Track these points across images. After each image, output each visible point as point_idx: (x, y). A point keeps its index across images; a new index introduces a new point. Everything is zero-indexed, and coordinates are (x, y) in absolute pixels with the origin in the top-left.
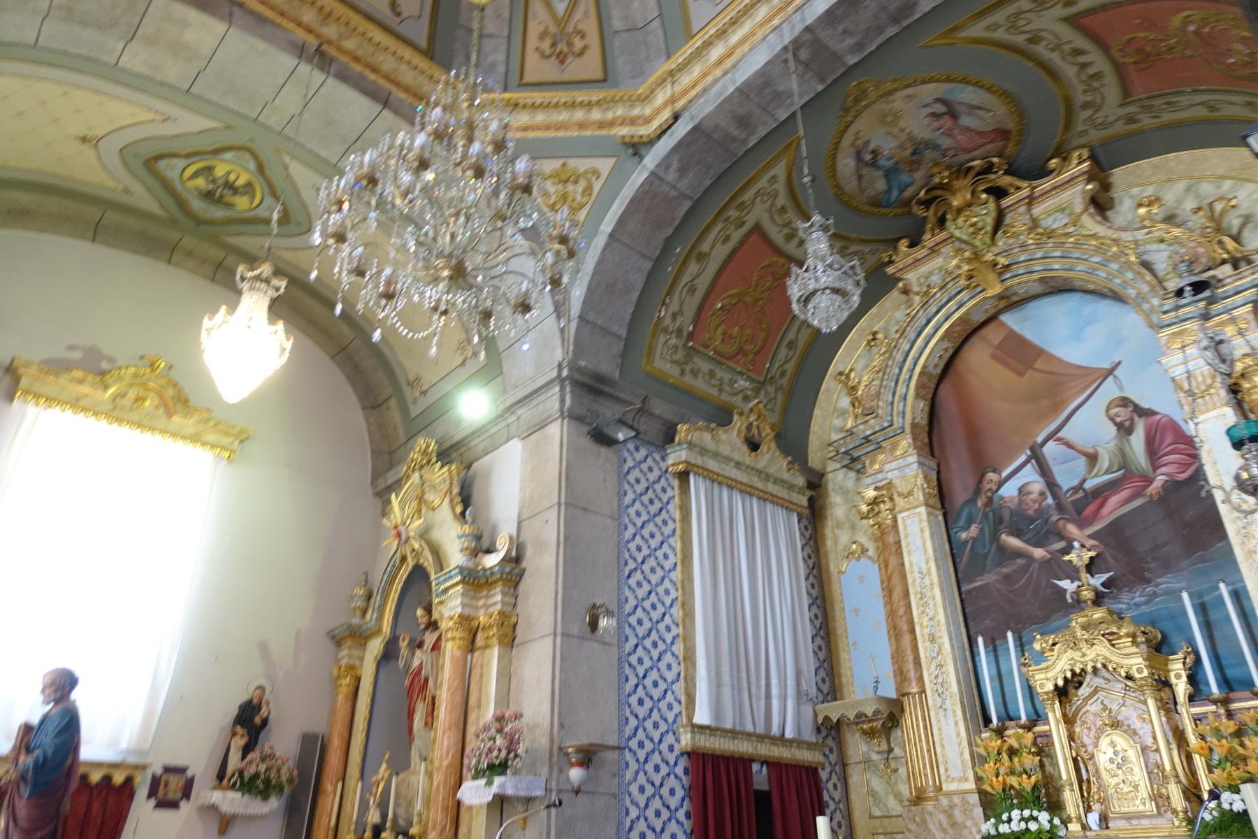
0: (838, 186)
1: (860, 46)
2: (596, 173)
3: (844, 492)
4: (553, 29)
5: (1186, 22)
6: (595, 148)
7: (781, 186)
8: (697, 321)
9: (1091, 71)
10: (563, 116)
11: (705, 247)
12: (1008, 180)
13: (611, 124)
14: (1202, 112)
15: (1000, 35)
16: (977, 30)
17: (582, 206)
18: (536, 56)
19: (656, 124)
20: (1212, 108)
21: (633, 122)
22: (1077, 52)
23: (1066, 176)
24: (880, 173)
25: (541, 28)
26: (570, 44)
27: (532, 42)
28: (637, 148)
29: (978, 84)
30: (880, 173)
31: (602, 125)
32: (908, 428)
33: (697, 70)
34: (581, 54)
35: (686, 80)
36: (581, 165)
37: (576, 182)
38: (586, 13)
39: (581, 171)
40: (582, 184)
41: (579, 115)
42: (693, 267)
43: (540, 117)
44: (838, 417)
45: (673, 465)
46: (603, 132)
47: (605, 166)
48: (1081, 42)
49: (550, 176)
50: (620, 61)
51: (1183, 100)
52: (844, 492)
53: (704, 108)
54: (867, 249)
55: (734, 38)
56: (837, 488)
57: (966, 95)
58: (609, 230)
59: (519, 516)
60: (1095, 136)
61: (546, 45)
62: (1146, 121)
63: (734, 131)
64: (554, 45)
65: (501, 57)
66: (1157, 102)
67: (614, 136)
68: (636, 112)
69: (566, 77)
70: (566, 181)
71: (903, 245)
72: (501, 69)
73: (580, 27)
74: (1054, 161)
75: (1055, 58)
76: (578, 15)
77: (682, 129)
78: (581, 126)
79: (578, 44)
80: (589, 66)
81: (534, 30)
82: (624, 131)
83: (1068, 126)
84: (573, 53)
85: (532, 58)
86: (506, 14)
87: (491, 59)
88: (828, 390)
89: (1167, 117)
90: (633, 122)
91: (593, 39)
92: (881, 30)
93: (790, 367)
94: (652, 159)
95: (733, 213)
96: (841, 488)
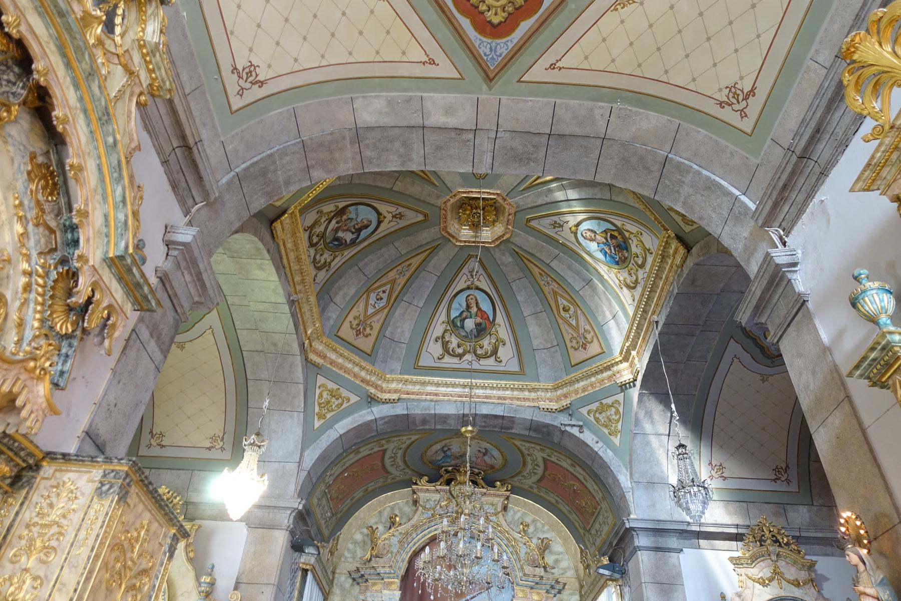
0: (426, 452)
1: (485, 427)
2: (349, 400)
3: (343, 589)
4: (362, 317)
5: (574, 485)
6: (355, 390)
7: (408, 442)
8: (334, 480)
9: (535, 471)
10: (350, 366)
11: (361, 450)
12: (482, 482)
13: (367, 383)
14: (554, 501)
15: (523, 448)
16: (518, 443)
17: (333, 410)
18: (349, 325)
19: (387, 396)
21: (376, 387)
22: (537, 465)
23: (500, 493)
24: (443, 455)
25: (358, 314)
26: (364, 329)
27: (350, 317)
28: (372, 400)
29: (501, 453)
30: (443, 455)
31: (363, 380)
32: (400, 577)
33: (417, 388)
34: (367, 336)
35: (410, 387)
36: (344, 393)
37: (337, 399)
38: (378, 320)
39: (343, 395)
40: (340, 401)
41: (356, 369)
42: (352, 456)
43: (340, 360)
44: (352, 543)
45: (304, 563)
46: (364, 385)
47: (354, 399)
48: (541, 464)
49: (329, 391)
50: (381, 350)
52: (343, 589)
53: (417, 411)
54: (410, 473)
55: (443, 390)
56: (339, 584)
57: (496, 453)
58: (342, 432)
59: (237, 579)
60: (517, 484)
61: (355, 323)
62: (535, 491)
63: (417, 422)
64: (358, 325)
65: (334, 316)
67: (368, 391)
68: (379, 383)
69: (355, 343)
70: (334, 396)
71: (426, 478)
72: (332, 322)
73: (373, 324)
74: (498, 483)
75: (530, 462)
76: (375, 319)
77: (400, 410)
78: (355, 376)
79: (368, 331)
80: (366, 344)
81: (354, 312)
82: (372, 390)
83: (512, 477)
84: (363, 334)
85: (346, 325)
86: (347, 299)
87: (330, 314)
88: (351, 525)
89: (542, 494)
90: (376, 387)
91: (375, 333)
92: (495, 427)
93: (345, 509)
94: (379, 411)
95: (383, 442)
96: (341, 585)
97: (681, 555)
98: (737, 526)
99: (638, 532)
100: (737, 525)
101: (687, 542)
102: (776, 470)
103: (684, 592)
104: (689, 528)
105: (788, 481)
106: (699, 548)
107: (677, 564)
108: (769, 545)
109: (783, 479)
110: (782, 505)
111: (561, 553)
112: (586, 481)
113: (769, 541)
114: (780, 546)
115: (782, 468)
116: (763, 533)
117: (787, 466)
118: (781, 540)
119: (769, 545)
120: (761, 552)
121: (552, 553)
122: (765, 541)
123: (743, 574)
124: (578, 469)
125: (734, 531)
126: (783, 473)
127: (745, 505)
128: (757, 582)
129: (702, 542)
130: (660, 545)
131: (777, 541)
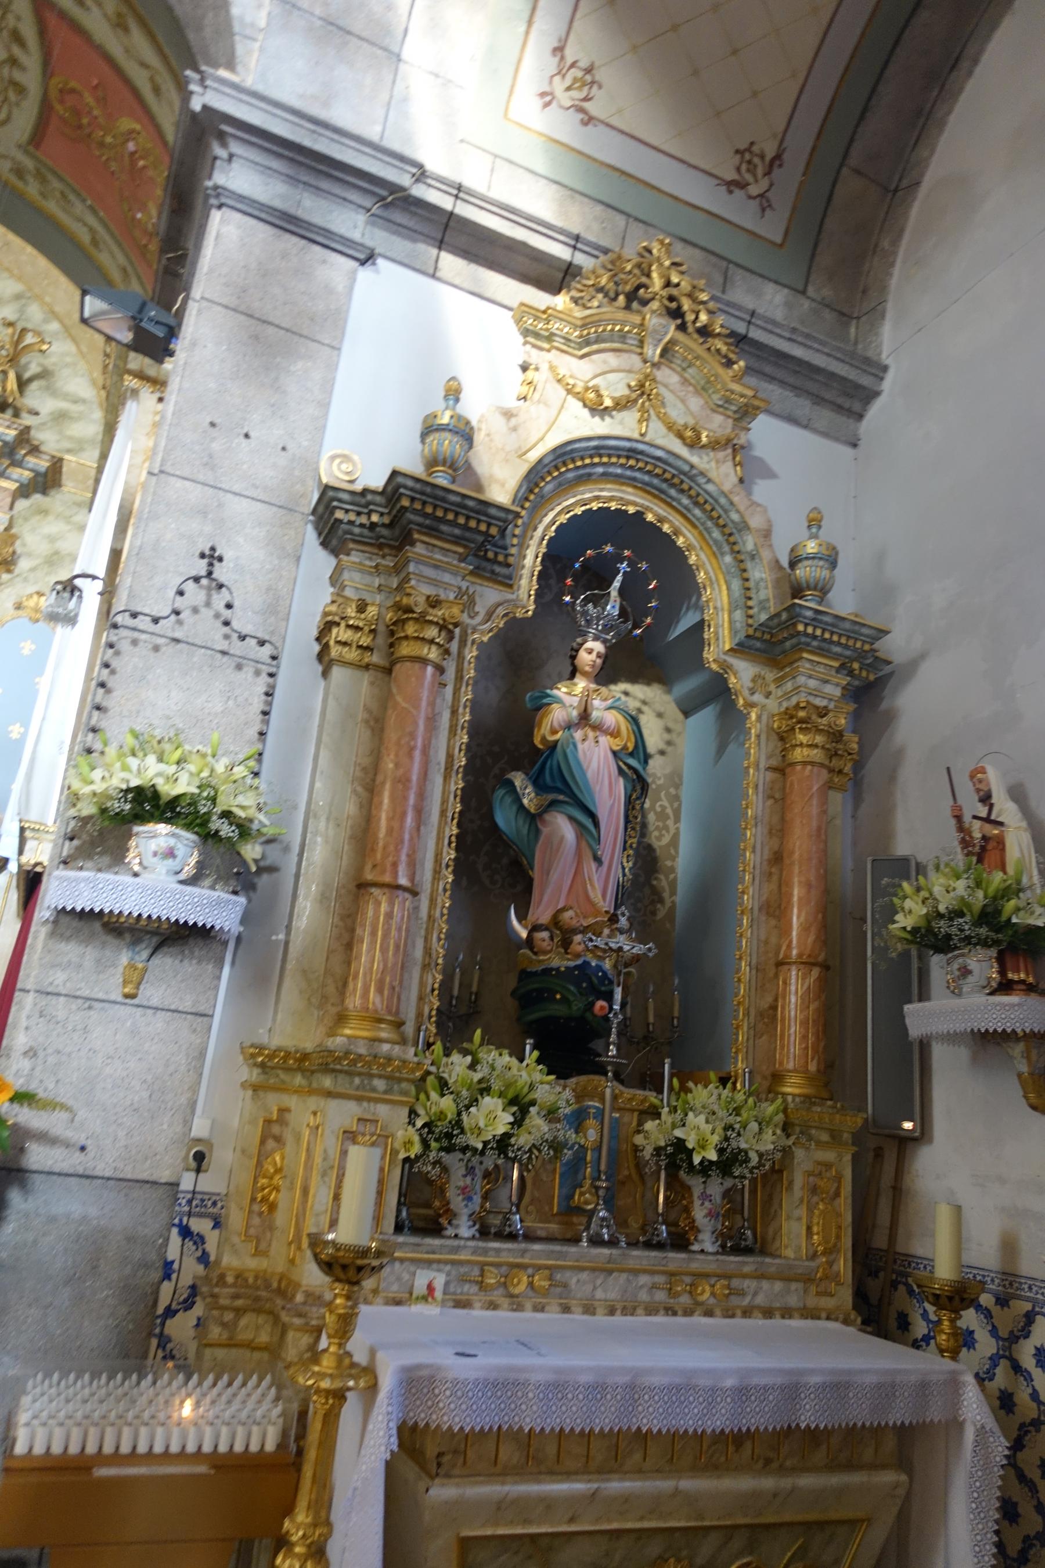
5: (130, 135)
14: (85, 238)
20: (95, 242)
51: (79, 208)
62: (32, 189)
66: (56, 184)
89: (52, 207)
97: (364, 274)
98: (576, 241)
99: (235, 147)
100: (577, 238)
101: (400, 245)
102: (745, 154)
103: (332, 367)
104: (419, 191)
105: (764, 202)
106: (433, 276)
107: (340, 288)
108: (653, 312)
109: (754, 190)
110: (724, 264)
111: (84, 401)
112: (157, 90)
113: (655, 305)
114: (682, 328)
115: (762, 157)
116: (644, 280)
117: (778, 157)
118: (690, 317)
119: (653, 312)
120: (623, 323)
121: (52, 391)
122: (645, 303)
123: (544, 367)
124: (138, 38)
125: (560, 251)
126: (760, 171)
127: (620, 221)
128: (576, 395)
129: (450, 263)
130: (300, 213)
131: (676, 314)
